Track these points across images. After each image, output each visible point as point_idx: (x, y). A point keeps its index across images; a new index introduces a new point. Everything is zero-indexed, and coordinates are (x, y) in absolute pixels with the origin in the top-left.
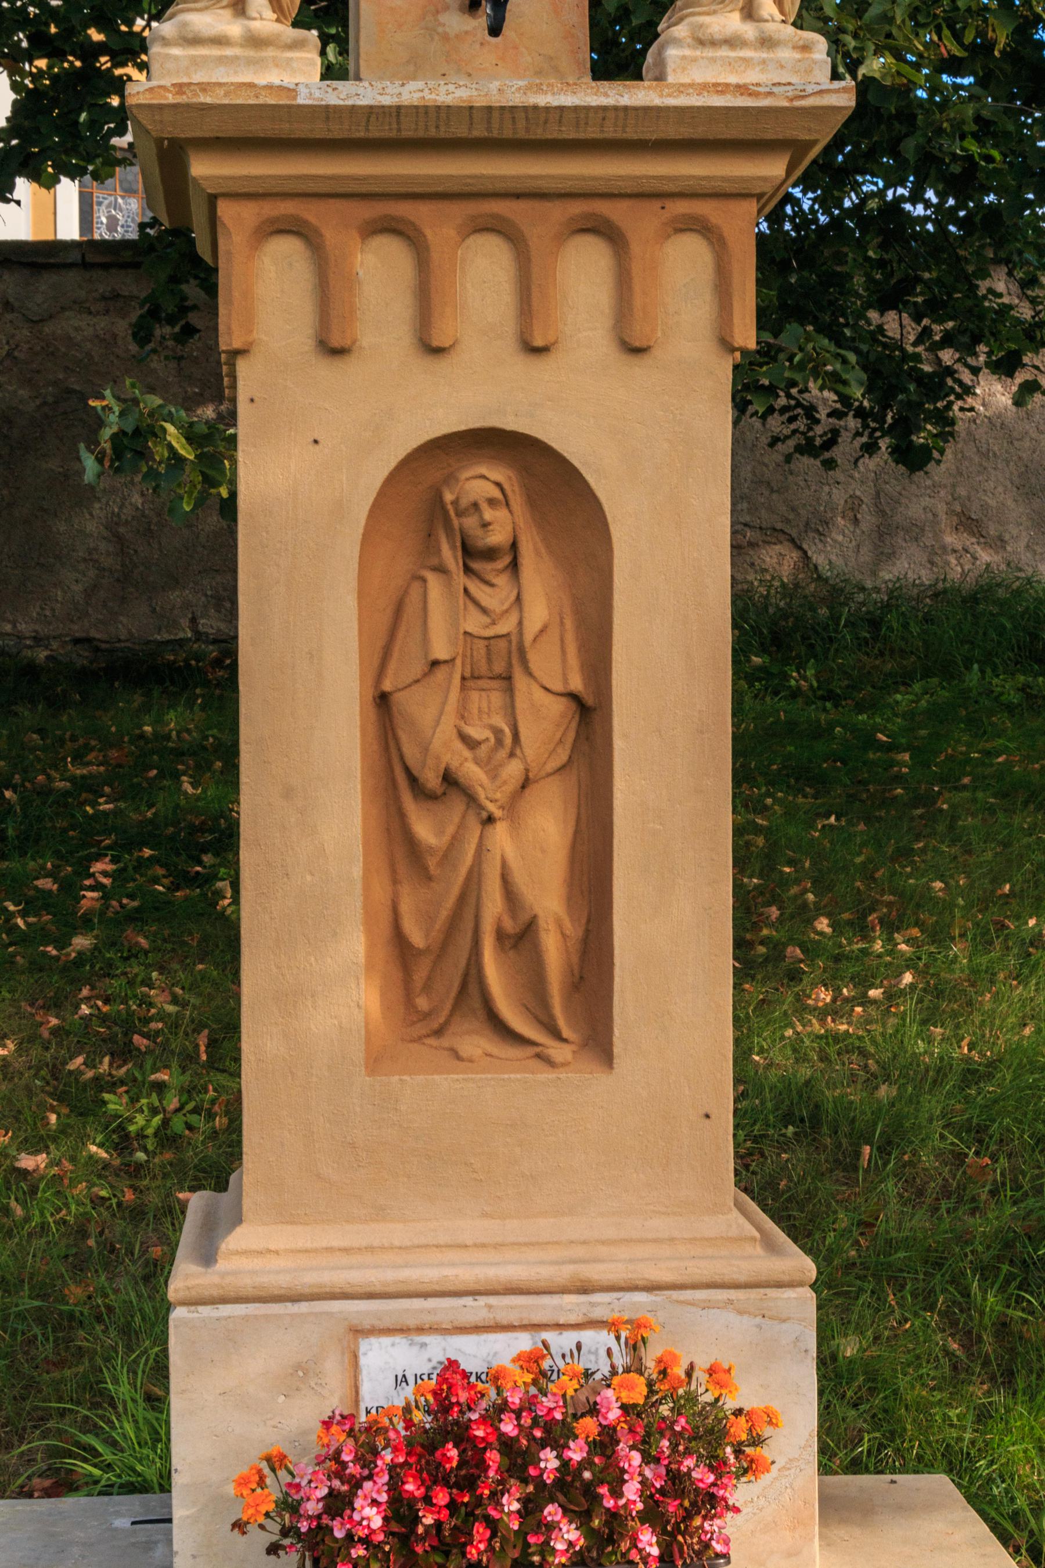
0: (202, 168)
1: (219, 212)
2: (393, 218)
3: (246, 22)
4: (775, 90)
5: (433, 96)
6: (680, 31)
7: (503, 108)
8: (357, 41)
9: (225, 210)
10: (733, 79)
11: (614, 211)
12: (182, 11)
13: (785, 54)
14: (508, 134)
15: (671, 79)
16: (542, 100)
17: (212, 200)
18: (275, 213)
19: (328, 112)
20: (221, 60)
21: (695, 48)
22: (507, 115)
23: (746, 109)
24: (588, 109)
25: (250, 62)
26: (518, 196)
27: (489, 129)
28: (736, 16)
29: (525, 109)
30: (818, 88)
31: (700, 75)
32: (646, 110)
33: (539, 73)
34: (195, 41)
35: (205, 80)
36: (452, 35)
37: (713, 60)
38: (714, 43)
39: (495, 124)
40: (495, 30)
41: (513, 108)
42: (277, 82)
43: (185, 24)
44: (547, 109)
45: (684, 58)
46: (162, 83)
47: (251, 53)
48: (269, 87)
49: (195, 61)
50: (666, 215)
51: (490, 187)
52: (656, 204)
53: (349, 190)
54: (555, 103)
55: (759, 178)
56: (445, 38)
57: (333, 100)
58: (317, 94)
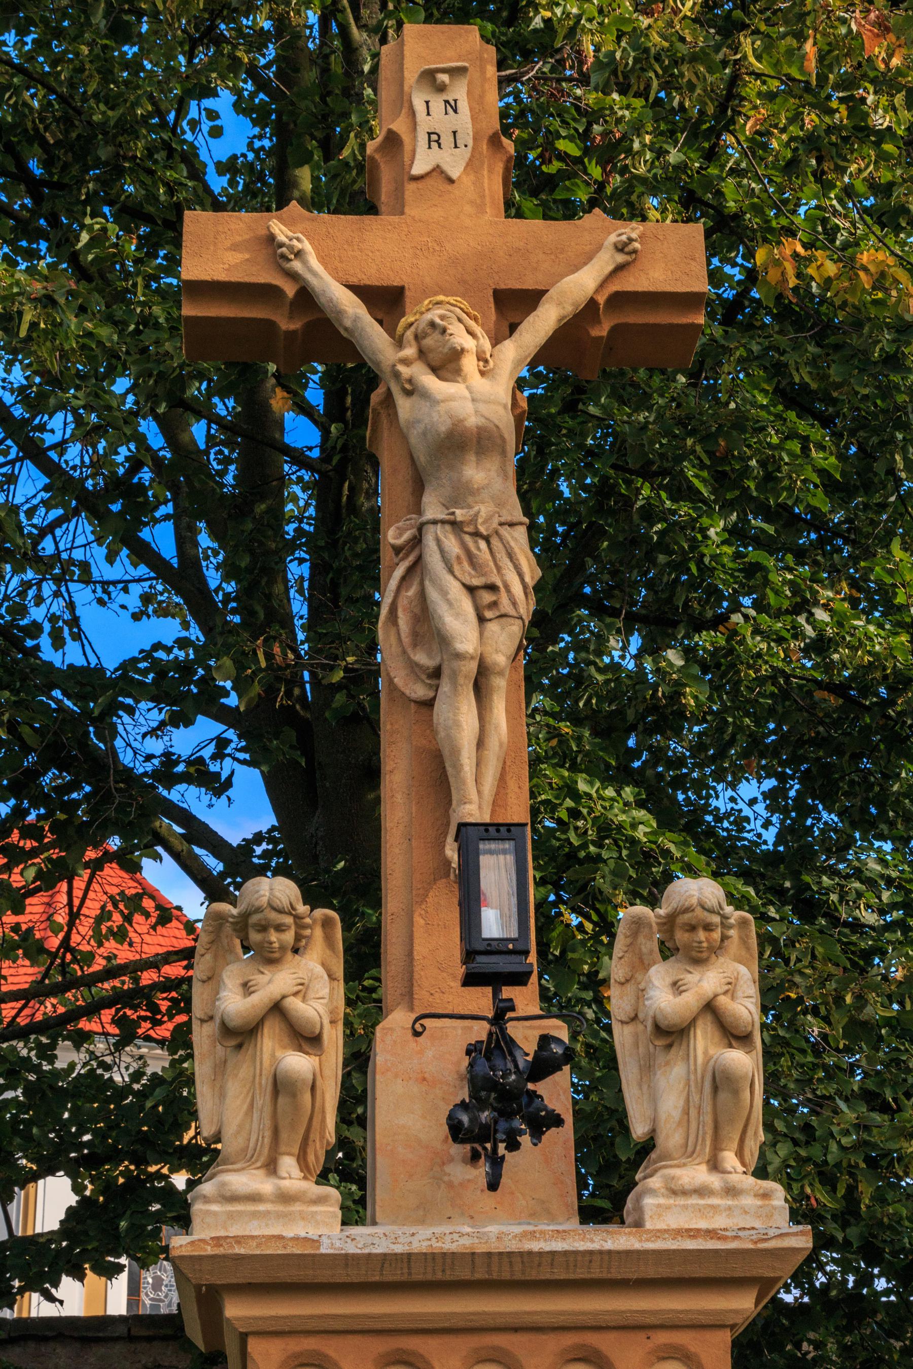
0: (235, 1310)
1: (249, 1349)
2: (404, 1351)
3: (277, 1181)
4: (741, 1234)
5: (439, 1244)
6: (655, 1182)
7: (501, 1254)
8: (374, 1189)
9: (254, 1346)
10: (703, 1224)
11: (603, 1342)
12: (222, 1171)
13: (748, 1201)
14: (506, 1276)
15: (649, 1225)
16: (536, 1246)
17: (244, 1337)
18: (297, 1349)
19: (347, 1260)
20: (255, 1215)
21: (668, 1197)
22: (506, 1260)
23: (716, 1251)
24: (576, 1253)
25: (279, 1216)
26: (516, 1330)
27: (489, 1272)
28: (704, 1168)
29: (521, 1254)
30: (779, 1232)
31: (674, 1221)
32: (628, 1253)
33: (533, 1215)
34: (234, 1198)
35: (240, 1233)
36: (456, 1183)
37: (685, 1207)
38: (685, 1193)
39: (495, 1268)
40: (493, 1185)
41: (510, 1254)
42: (303, 1234)
43: (224, 1184)
44: (540, 1254)
45: (659, 1206)
46: (202, 1236)
47: (280, 1208)
48: (296, 1239)
49: (231, 1215)
50: (650, 1345)
51: (491, 1323)
52: (641, 1336)
53: (366, 1327)
54: (547, 1249)
55: (731, 1311)
56: (450, 1185)
57: (351, 1249)
58: (338, 1244)
